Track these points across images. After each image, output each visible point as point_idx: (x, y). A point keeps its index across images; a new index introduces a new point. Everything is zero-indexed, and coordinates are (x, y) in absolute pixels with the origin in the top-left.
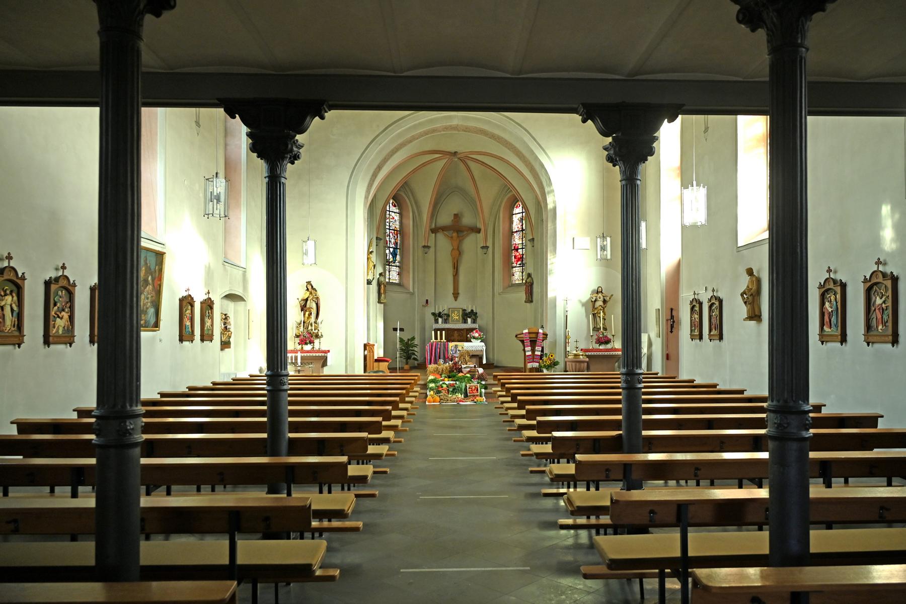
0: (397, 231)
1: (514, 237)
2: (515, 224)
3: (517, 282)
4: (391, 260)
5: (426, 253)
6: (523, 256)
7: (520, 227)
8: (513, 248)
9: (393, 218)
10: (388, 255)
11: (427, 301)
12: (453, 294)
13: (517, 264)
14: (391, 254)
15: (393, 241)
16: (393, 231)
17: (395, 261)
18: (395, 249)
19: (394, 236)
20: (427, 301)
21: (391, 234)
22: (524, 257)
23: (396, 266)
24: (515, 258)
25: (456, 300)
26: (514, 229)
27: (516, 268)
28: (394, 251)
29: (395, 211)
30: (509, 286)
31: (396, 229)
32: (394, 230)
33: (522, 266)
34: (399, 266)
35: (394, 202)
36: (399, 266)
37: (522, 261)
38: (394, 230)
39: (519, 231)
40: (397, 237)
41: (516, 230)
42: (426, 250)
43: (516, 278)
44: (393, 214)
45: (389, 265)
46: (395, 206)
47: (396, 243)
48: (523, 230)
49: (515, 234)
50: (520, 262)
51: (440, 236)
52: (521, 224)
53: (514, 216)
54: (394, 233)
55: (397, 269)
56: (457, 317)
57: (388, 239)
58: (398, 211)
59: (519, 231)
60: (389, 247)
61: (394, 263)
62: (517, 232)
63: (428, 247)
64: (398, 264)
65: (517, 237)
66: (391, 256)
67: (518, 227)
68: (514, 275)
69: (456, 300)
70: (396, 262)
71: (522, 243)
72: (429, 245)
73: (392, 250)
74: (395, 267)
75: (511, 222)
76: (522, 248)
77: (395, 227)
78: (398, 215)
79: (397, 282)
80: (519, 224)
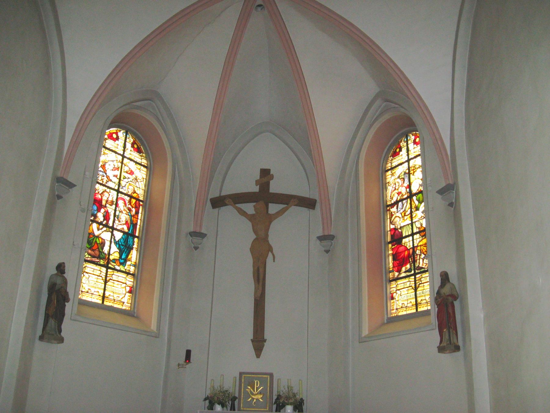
0: (137, 199)
1: (392, 215)
2: (390, 189)
3: (402, 313)
4: (115, 255)
5: (196, 248)
6: (414, 252)
7: (403, 190)
8: (389, 239)
9: (132, 173)
10: (107, 244)
11: (188, 353)
12: (253, 341)
13: (399, 271)
14: (116, 243)
15: (124, 217)
16: (127, 198)
17: (126, 260)
18: (129, 235)
19: (130, 210)
20: (188, 353)
21: (121, 203)
22: (418, 252)
23: (128, 273)
24: (394, 259)
25: (258, 356)
26: (389, 198)
27: (399, 282)
28: (126, 241)
29: (139, 160)
30: (383, 324)
31: (135, 195)
32: (131, 197)
33: (415, 274)
34: (133, 275)
35: (138, 142)
36: (133, 275)
37: (414, 261)
38: (131, 197)
39: (401, 200)
40: (137, 213)
41: (394, 200)
42: (196, 240)
43: (400, 304)
44: (132, 165)
45: (107, 268)
46: (139, 150)
47: (132, 225)
48: (411, 196)
49: (394, 210)
50: (408, 266)
51: (229, 212)
52: (406, 184)
53: (389, 172)
54: (130, 202)
55: (130, 281)
56: (260, 396)
57: (111, 209)
58: (144, 162)
59: (401, 200)
60: (113, 228)
61: (123, 264)
62: (397, 203)
63: (203, 236)
64: (132, 269)
65: (398, 214)
66: (114, 248)
67: (399, 193)
68: (392, 298)
69: (258, 356)
70: (128, 263)
71: (412, 224)
72: (203, 231)
73: (118, 236)
74: (124, 275)
75: (384, 185)
76: (413, 234)
77: (135, 192)
78: (145, 169)
79: (126, 307)
80: (402, 186)
